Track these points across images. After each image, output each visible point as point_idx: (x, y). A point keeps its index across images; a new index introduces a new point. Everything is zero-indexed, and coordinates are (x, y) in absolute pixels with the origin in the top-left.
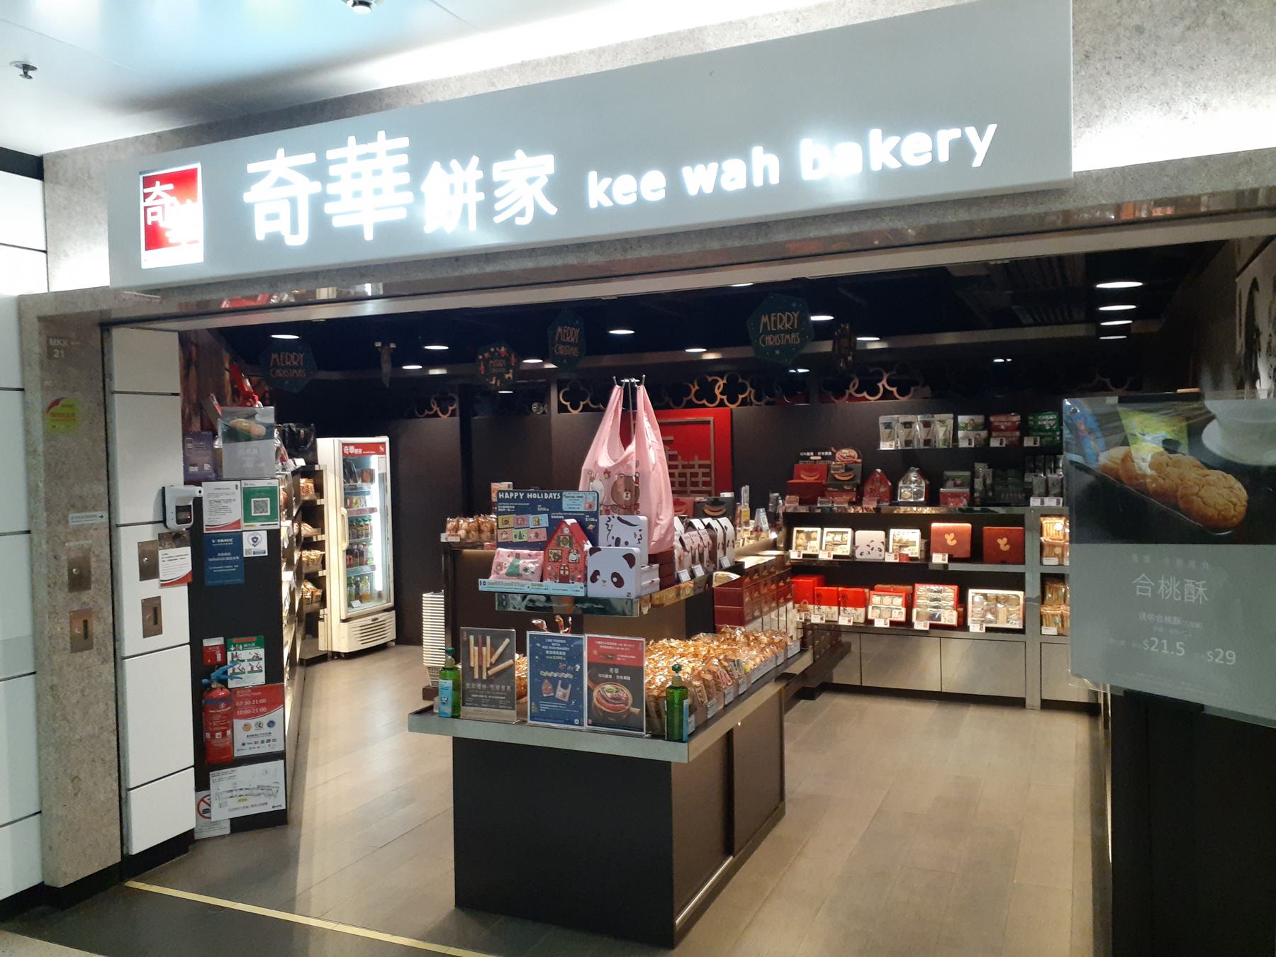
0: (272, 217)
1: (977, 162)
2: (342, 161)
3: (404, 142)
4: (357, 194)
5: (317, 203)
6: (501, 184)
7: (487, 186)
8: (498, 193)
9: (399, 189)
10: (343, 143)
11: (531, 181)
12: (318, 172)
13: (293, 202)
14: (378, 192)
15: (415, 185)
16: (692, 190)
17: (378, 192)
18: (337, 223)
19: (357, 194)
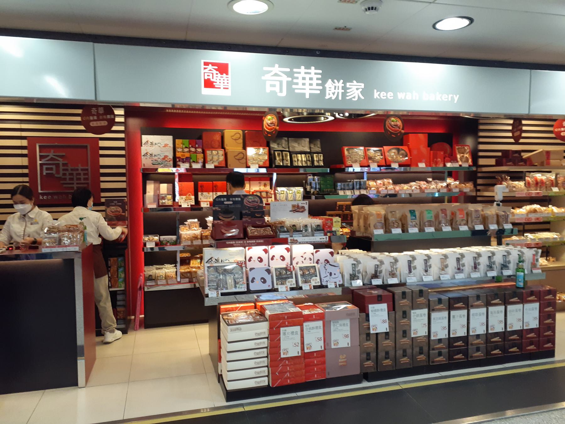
0: (274, 86)
3: (320, 71)
4: (304, 84)
5: (289, 84)
6: (349, 88)
7: (345, 88)
8: (348, 91)
9: (318, 85)
10: (300, 68)
12: (291, 74)
13: (281, 83)
14: (311, 85)
15: (323, 84)
16: (399, 98)
17: (311, 85)
18: (297, 91)
19: (304, 84)
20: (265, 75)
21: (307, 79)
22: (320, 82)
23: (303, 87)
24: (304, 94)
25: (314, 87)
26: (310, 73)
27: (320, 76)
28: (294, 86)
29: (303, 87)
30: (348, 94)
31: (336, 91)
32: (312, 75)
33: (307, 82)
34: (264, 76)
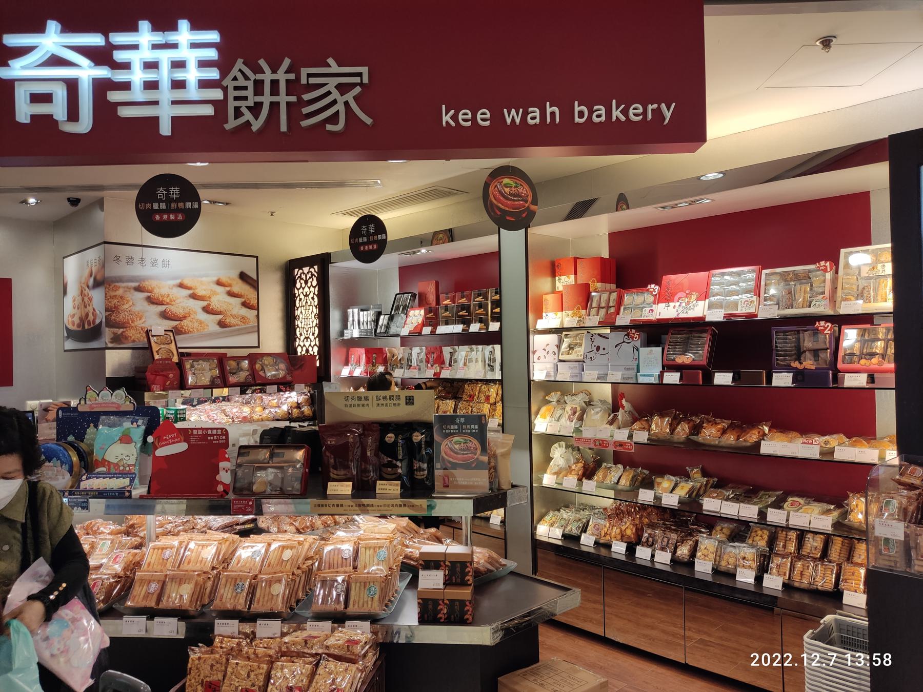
1: (667, 121)
2: (135, 47)
4: (151, 86)
10: (134, 29)
11: (343, 89)
12: (100, 56)
13: (72, 86)
17: (179, 85)
20: (10, 62)
21: (165, 67)
22: (213, 74)
23: (151, 95)
24: (155, 120)
25: (193, 92)
26: (174, 46)
27: (211, 54)
28: (114, 96)
29: (151, 95)
30: (305, 110)
31: (266, 99)
32: (183, 54)
33: (164, 75)
34: (8, 65)
